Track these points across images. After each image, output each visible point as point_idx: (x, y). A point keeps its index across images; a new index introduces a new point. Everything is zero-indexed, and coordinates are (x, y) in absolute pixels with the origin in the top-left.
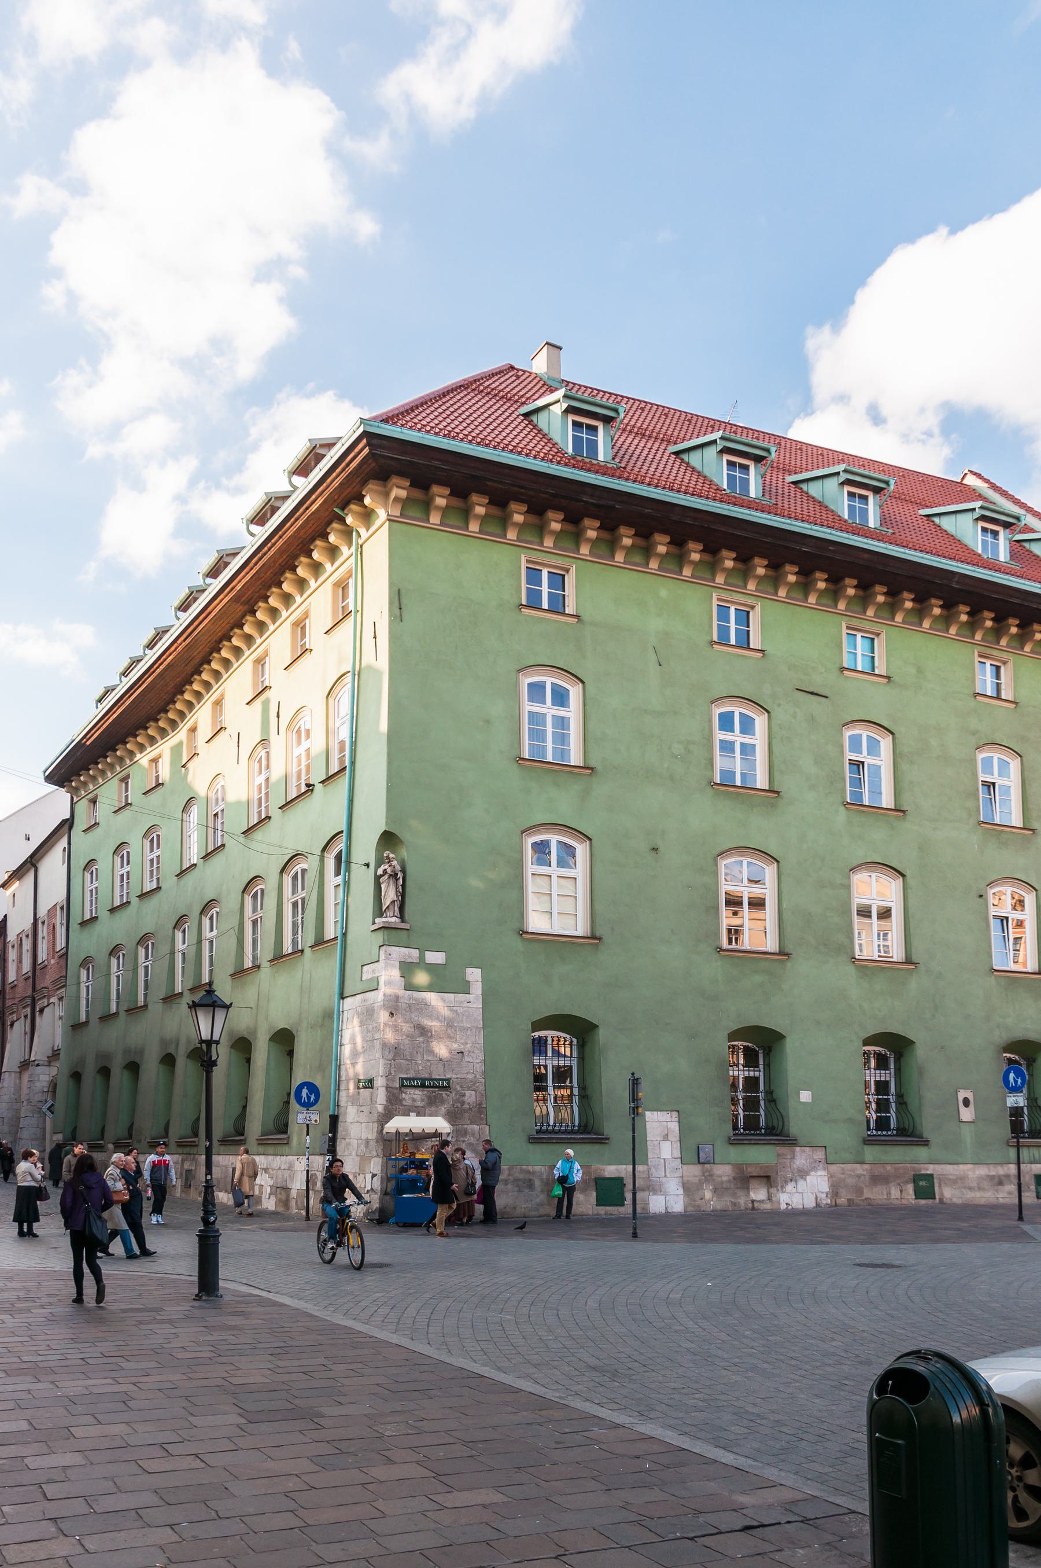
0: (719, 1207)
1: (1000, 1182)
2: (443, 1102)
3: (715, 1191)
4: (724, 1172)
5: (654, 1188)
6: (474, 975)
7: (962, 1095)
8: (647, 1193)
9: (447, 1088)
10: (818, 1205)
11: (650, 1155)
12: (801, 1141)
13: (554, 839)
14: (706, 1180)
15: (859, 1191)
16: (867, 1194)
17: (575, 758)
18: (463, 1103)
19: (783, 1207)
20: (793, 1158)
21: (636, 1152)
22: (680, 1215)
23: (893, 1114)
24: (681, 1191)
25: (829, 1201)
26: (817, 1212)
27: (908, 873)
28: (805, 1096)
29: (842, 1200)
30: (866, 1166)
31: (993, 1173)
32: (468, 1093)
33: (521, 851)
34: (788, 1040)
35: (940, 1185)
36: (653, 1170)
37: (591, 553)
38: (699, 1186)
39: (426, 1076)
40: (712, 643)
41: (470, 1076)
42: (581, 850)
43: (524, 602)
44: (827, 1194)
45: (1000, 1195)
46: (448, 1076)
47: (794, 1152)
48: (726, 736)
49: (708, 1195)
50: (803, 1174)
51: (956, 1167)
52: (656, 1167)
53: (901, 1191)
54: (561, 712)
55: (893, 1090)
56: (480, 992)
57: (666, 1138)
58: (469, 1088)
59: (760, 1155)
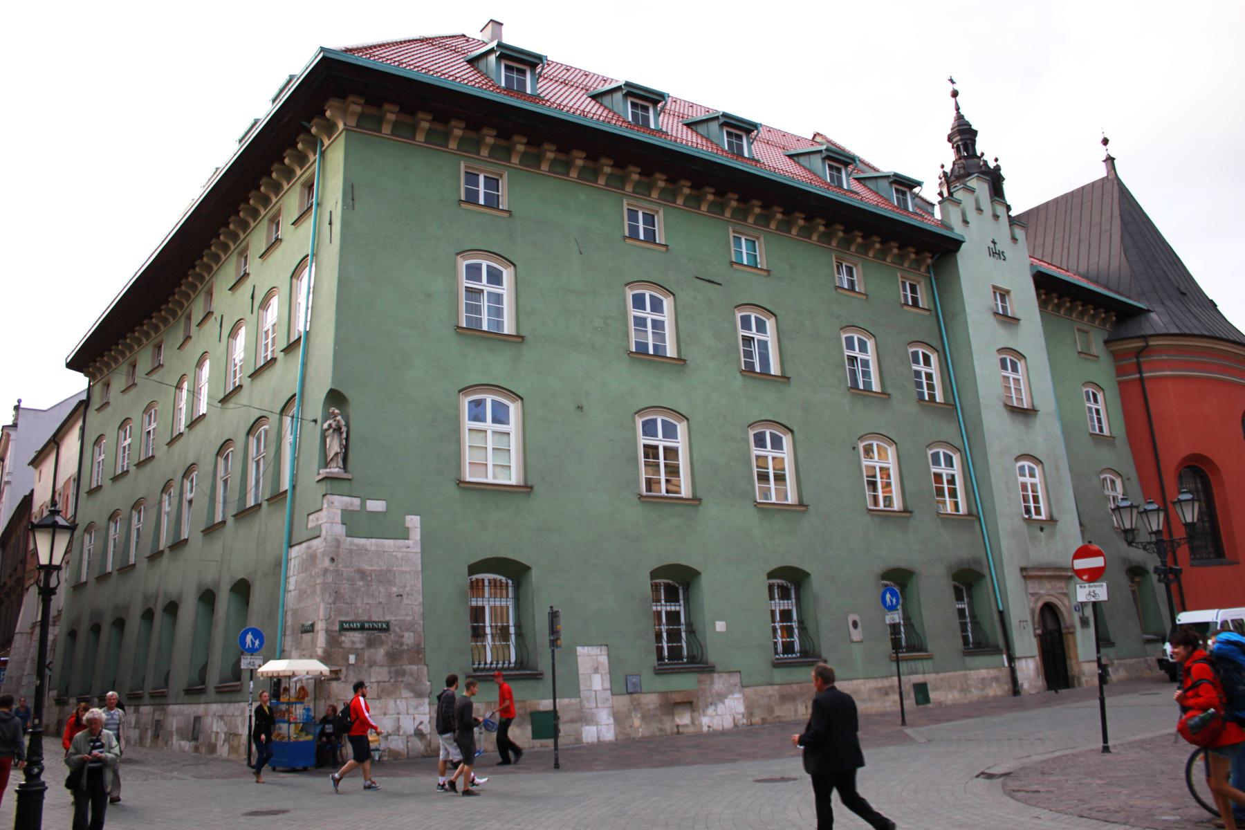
0: (647, 734)
1: (886, 692)
2: (382, 643)
3: (643, 718)
4: (650, 700)
6: (413, 521)
7: (851, 618)
9: (387, 630)
10: (736, 726)
11: (582, 688)
12: (718, 668)
13: (489, 399)
14: (635, 709)
15: (771, 710)
16: (778, 712)
17: (508, 328)
18: (402, 644)
19: (705, 729)
20: (712, 683)
22: (611, 743)
23: (796, 639)
24: (612, 721)
26: (736, 731)
28: (720, 626)
29: (756, 720)
30: (776, 687)
31: (880, 685)
32: (406, 635)
33: (457, 408)
34: (703, 576)
36: (585, 702)
37: (521, 163)
38: (628, 716)
39: (366, 618)
40: (625, 237)
41: (409, 618)
42: (514, 409)
43: (463, 198)
45: (888, 704)
46: (387, 618)
48: (639, 313)
49: (637, 722)
50: (721, 697)
52: (588, 699)
54: (495, 289)
55: (795, 617)
56: (418, 537)
57: (596, 670)
58: (408, 630)
59: (682, 683)
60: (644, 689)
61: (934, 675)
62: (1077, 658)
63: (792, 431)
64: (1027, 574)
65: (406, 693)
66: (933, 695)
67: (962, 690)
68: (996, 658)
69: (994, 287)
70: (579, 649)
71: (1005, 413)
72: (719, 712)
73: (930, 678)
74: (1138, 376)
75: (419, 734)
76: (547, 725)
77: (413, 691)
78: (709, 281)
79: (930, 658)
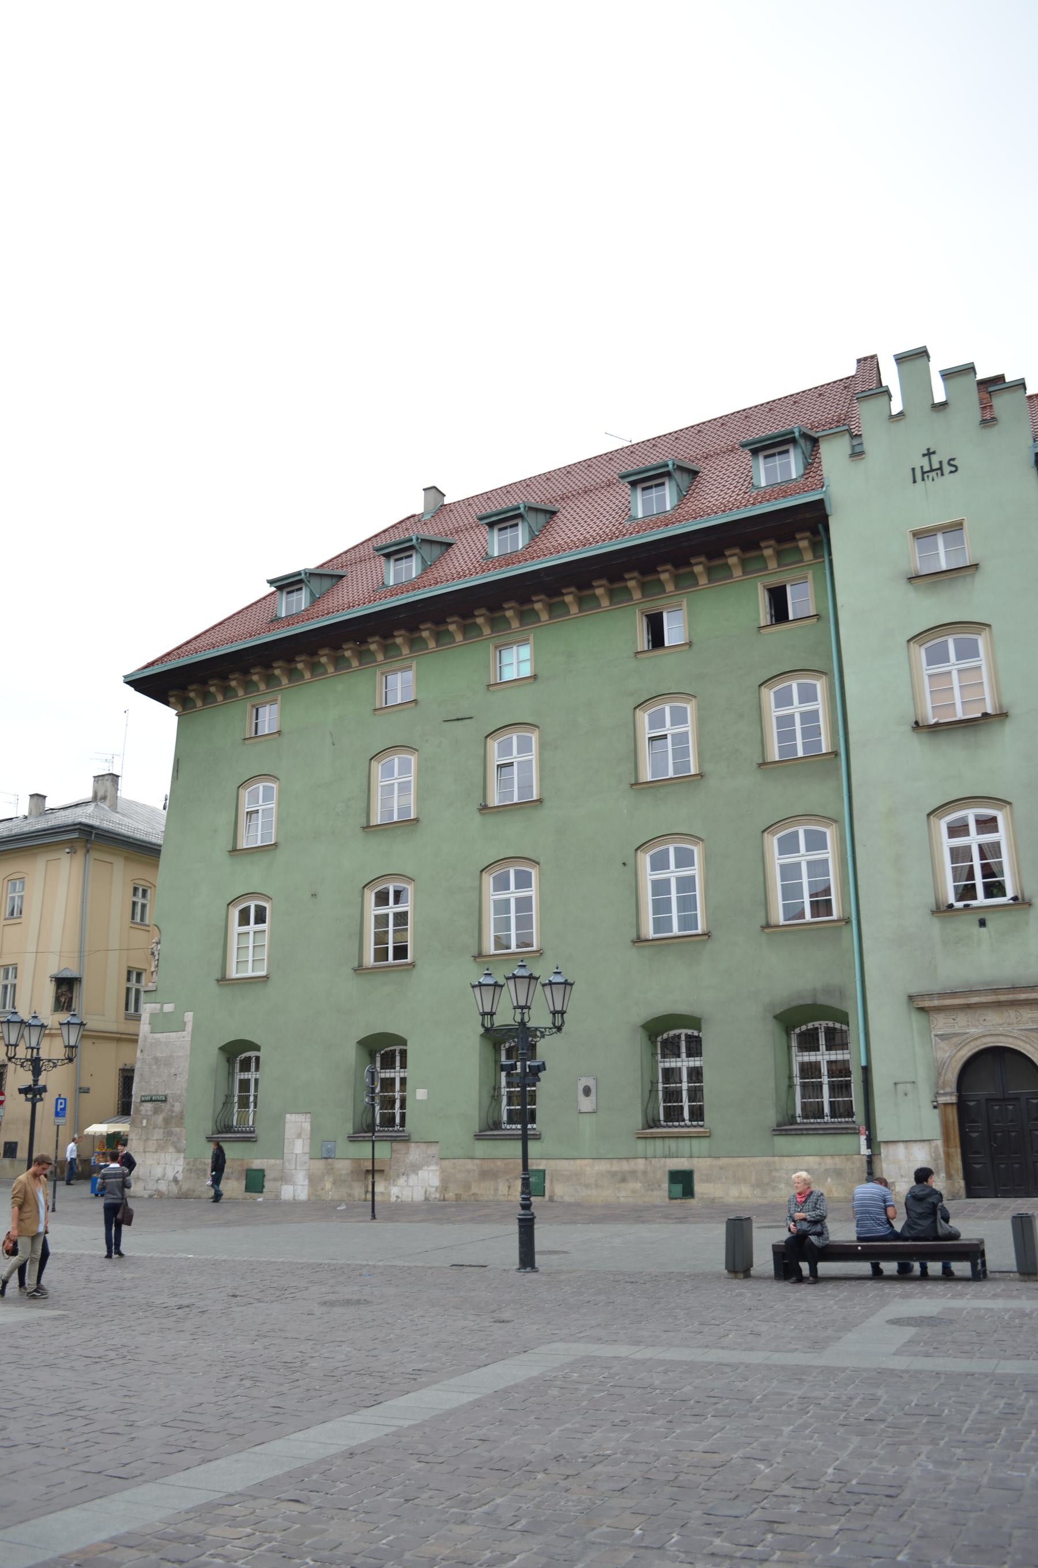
0: (336, 1198)
2: (162, 1112)
3: (334, 1183)
4: (343, 1166)
5: (284, 1178)
6: (189, 1016)
8: (279, 1183)
9: (165, 1101)
10: (426, 1199)
12: (414, 1138)
15: (467, 1186)
16: (475, 1189)
18: (173, 1112)
19: (393, 1199)
21: (278, 1149)
24: (306, 1182)
25: (438, 1195)
27: (542, 861)
30: (477, 1162)
32: (176, 1104)
35: (552, 1181)
36: (287, 1164)
44: (437, 1188)
45: (623, 1194)
47: (408, 1148)
49: (328, 1186)
50: (415, 1168)
51: (572, 1162)
53: (509, 1187)
57: (299, 1136)
61: (709, 1161)
63: (538, 863)
65: (171, 1149)
66: (698, 1188)
67: (759, 1184)
68: (844, 1142)
69: (917, 535)
70: (288, 1116)
71: (917, 744)
72: (411, 1183)
73: (700, 1166)
75: (175, 1180)
76: (255, 1181)
77: (175, 1147)
78: (458, 720)
79: (707, 1136)
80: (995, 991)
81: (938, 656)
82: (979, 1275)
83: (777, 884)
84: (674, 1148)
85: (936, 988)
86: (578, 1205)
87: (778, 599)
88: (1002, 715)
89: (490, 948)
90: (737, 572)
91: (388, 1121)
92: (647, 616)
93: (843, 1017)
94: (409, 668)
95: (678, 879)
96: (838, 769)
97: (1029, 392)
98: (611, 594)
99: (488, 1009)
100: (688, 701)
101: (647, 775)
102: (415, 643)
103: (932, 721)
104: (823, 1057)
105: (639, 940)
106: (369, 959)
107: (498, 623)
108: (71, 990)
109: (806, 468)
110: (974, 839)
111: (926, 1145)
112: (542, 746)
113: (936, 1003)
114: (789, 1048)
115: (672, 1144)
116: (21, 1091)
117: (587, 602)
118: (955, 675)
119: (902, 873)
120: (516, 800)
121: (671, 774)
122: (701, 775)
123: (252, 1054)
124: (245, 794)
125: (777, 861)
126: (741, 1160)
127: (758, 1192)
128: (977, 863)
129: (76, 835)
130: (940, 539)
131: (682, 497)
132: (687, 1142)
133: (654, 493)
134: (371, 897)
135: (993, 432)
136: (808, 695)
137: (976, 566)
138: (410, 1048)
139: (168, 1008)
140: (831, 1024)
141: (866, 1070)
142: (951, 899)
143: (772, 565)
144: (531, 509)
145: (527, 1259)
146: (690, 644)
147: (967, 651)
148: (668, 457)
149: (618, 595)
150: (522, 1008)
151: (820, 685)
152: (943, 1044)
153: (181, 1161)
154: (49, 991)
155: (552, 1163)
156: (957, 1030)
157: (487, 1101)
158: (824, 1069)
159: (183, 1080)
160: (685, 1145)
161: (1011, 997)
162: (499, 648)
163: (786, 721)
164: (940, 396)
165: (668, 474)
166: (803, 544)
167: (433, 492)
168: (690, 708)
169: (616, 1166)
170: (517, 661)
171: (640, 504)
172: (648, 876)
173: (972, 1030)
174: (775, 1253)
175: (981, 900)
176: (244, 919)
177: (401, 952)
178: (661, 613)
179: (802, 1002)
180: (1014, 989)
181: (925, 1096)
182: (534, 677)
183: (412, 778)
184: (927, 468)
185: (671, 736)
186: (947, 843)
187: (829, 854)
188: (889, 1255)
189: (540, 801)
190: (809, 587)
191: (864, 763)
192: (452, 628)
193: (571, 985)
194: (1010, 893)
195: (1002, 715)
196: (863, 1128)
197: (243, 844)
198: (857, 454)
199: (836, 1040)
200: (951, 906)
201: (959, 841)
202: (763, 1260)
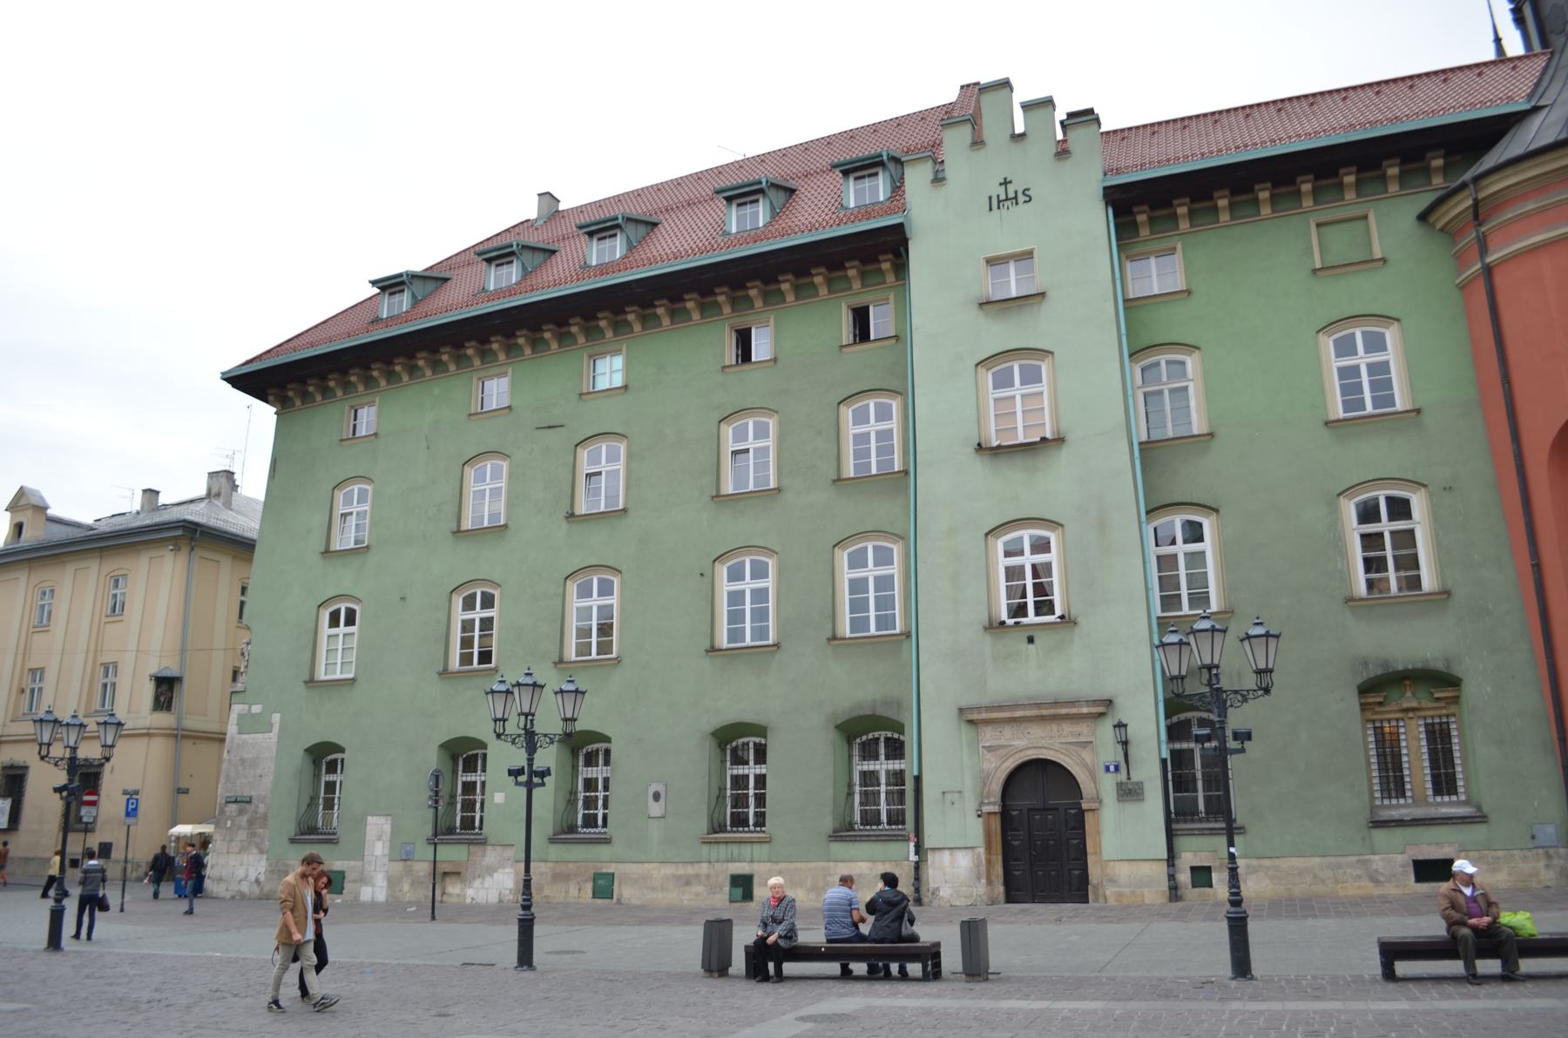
3: (412, 884)
5: (363, 880)
6: (276, 718)
9: (250, 802)
10: (500, 901)
12: (491, 840)
19: (468, 901)
21: (359, 852)
45: (686, 897)
49: (406, 887)
50: (491, 870)
57: (379, 838)
59: (451, 854)
60: (417, 857)
62: (1098, 852)
64: (972, 719)
65: (255, 851)
68: (894, 848)
69: (991, 262)
71: (979, 465)
73: (757, 869)
74: (1479, 265)
75: (257, 881)
79: (768, 841)
80: (1038, 705)
81: (1003, 381)
82: (934, 973)
83: (845, 597)
84: (736, 853)
85: (985, 702)
86: (642, 907)
87: (861, 318)
88: (1060, 440)
89: (571, 653)
90: (823, 291)
91: (468, 824)
92: (738, 331)
93: (900, 728)
94: (505, 374)
95: (753, 591)
96: (907, 487)
97: (1103, 129)
98: (702, 308)
99: (499, 715)
100: (771, 417)
101: (728, 488)
102: (511, 350)
103: (995, 444)
104: (883, 766)
105: (713, 649)
106: (455, 663)
107: (592, 332)
108: (171, 689)
109: (893, 191)
110: (1028, 560)
111: (969, 852)
112: (630, 456)
113: (984, 716)
114: (850, 757)
115: (735, 848)
116: (56, 790)
117: (678, 314)
118: (1018, 399)
119: (957, 588)
120: (602, 509)
121: (751, 487)
122: (778, 490)
123: (338, 756)
124: (340, 496)
125: (846, 574)
126: (799, 865)
127: (812, 896)
128: (1029, 581)
129: (179, 532)
130: (1012, 266)
131: (775, 214)
132: (748, 847)
133: (748, 209)
134: (458, 602)
135: (1067, 164)
136: (883, 414)
137: (1042, 294)
138: (489, 752)
139: (256, 709)
140: (889, 734)
141: (918, 780)
142: (1004, 616)
143: (857, 285)
144: (629, 219)
145: (525, 957)
146: (775, 360)
147: (1031, 376)
148: (763, 175)
149: (708, 309)
150: (526, 715)
151: (895, 405)
152: (989, 756)
153: (264, 863)
154: (149, 689)
155: (621, 866)
156: (1003, 742)
157: (562, 805)
158: (883, 780)
159: (268, 781)
160: (746, 850)
161: (1053, 711)
162: (594, 358)
163: (862, 439)
164: (1020, 128)
165: (761, 191)
166: (886, 266)
167: (548, 198)
168: (772, 423)
169: (682, 870)
170: (610, 371)
171: (734, 219)
172: (725, 587)
173: (1018, 743)
174: (747, 954)
175: (1031, 618)
176: (334, 621)
177: (485, 657)
178: (749, 330)
179: (861, 713)
180: (1056, 704)
181: (971, 806)
182: (625, 387)
183: (503, 484)
184: (1003, 197)
185: (754, 450)
186: (1003, 562)
187: (895, 570)
188: (859, 956)
189: (625, 510)
190: (890, 307)
191: (931, 483)
192: (547, 335)
193: (583, 693)
194: (1058, 612)
195: (1060, 440)
196: (912, 836)
197: (336, 545)
198: (938, 179)
199: (896, 749)
200: (1003, 623)
201: (1014, 561)
202: (739, 962)
